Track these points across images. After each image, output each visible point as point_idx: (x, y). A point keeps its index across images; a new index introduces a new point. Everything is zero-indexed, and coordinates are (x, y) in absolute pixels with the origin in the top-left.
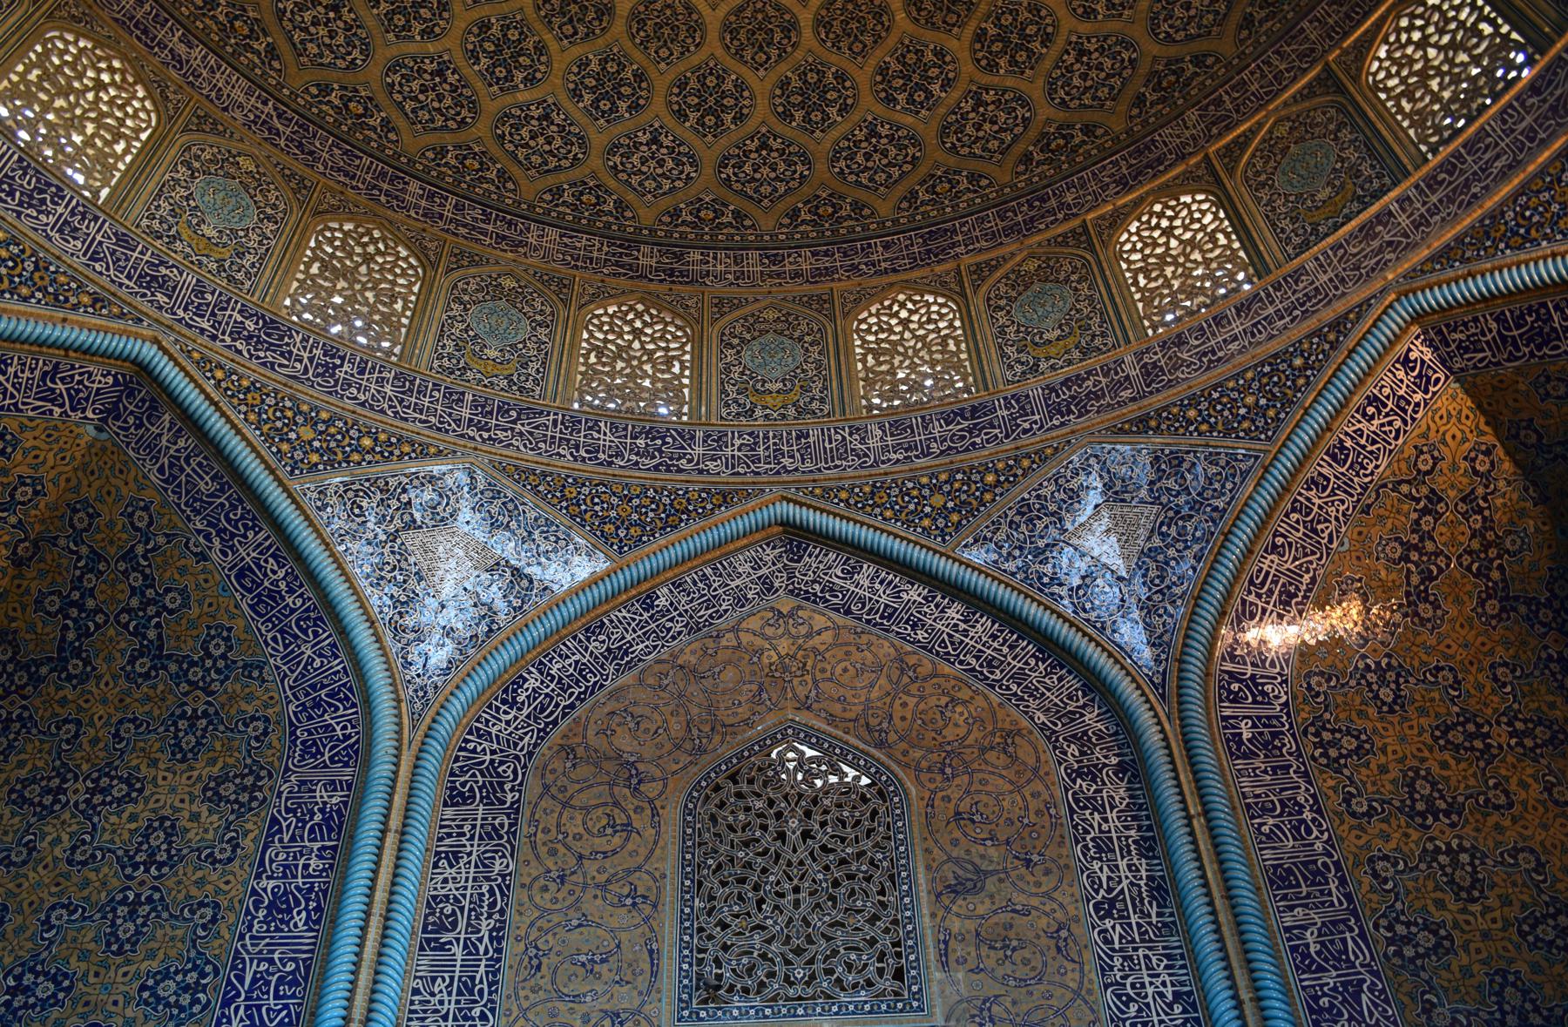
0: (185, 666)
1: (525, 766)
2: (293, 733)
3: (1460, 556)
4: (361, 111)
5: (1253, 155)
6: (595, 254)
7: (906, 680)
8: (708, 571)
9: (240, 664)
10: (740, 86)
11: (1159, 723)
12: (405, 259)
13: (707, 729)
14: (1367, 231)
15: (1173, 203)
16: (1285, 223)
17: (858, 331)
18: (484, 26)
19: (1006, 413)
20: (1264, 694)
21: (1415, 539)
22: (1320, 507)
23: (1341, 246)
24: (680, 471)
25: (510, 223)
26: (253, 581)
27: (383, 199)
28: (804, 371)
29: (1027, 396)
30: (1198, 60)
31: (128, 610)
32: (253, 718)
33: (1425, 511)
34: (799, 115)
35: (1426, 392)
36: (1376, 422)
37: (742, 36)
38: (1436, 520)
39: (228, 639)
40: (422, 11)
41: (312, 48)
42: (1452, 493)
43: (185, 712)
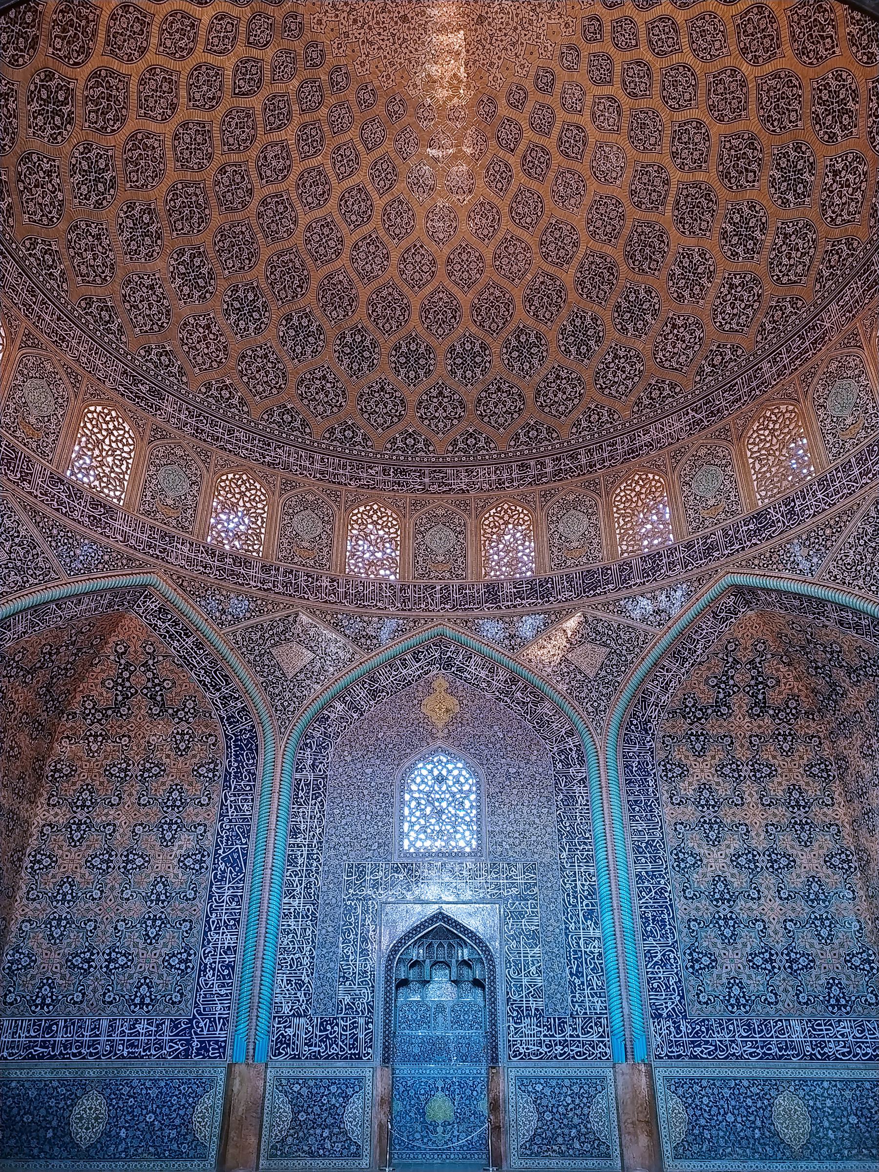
4: (720, 358)
18: (724, 234)
31: (830, 660)
40: (699, 271)
41: (682, 359)
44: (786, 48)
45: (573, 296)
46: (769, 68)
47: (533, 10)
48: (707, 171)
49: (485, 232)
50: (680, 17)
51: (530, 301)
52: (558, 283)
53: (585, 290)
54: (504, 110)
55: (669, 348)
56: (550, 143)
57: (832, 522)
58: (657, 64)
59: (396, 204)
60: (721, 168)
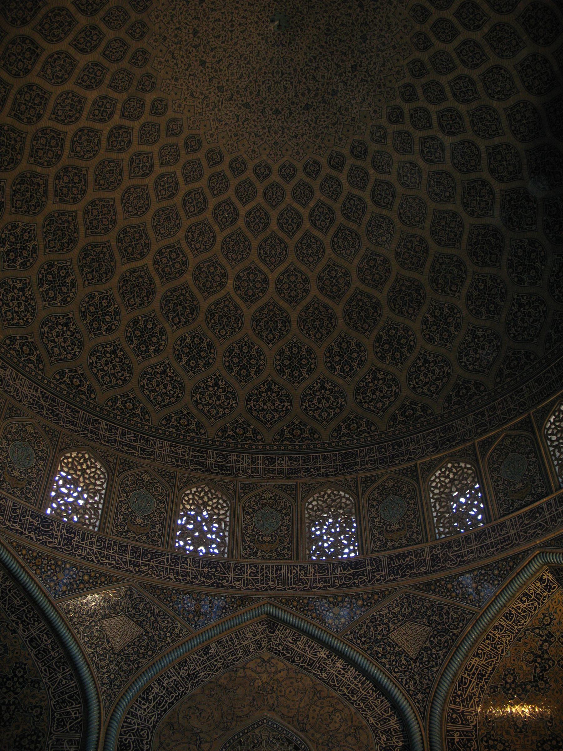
0: (5, 680)
1: (152, 732)
2: (53, 715)
3: (559, 661)
5: (493, 452)
6: (186, 457)
7: (316, 698)
8: (233, 636)
9: (30, 680)
10: (260, 353)
11: (420, 731)
12: (100, 469)
13: (230, 718)
14: (532, 514)
15: (456, 465)
16: (501, 495)
17: (308, 508)
18: (136, 322)
19: (370, 568)
20: (467, 720)
21: (540, 653)
22: (499, 638)
23: (521, 518)
24: (223, 586)
25: (147, 441)
26: (36, 644)
27: (89, 435)
28: (281, 531)
29: (380, 560)
30: (477, 385)
32: (35, 707)
33: (545, 641)
34: (287, 371)
35: (549, 592)
36: (526, 604)
37: (262, 324)
38: (550, 645)
39: (25, 669)
40: (106, 317)
42: (558, 634)
43: (5, 702)
44: (254, 307)
45: (40, 219)
46: (238, 300)
47: (215, 106)
48: (163, 284)
49: (60, 113)
50: (241, 223)
51: (22, 182)
52: (44, 199)
53: (49, 227)
54: (149, 98)
55: (54, 333)
56: (136, 147)
57: (93, 574)
58: (208, 215)
59: (68, 19)
60: (169, 294)
